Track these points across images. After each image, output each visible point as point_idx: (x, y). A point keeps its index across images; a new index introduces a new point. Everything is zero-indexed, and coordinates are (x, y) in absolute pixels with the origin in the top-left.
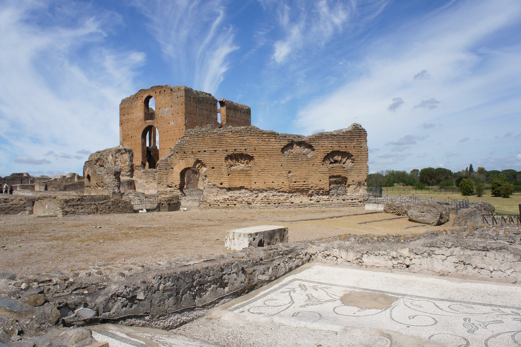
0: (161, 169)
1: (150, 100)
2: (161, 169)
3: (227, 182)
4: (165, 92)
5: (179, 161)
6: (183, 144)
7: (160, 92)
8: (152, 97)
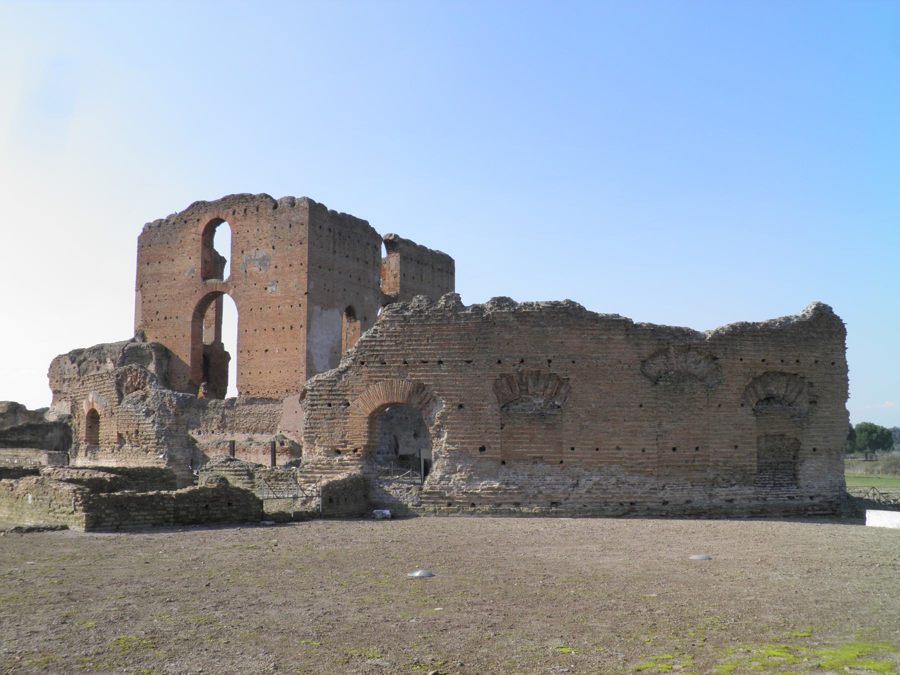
0: (317, 405)
1: (217, 229)
2: (317, 405)
3: (498, 446)
4: (258, 210)
5: (368, 386)
6: (381, 341)
7: (245, 210)
8: (223, 221)
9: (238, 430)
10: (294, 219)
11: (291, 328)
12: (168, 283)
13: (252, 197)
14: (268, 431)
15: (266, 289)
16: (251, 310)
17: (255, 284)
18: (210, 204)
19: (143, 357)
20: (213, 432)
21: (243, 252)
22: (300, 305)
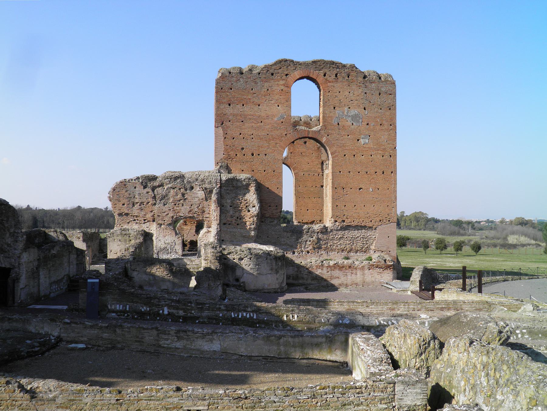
4: (348, 77)
7: (336, 75)
9: (332, 250)
10: (383, 89)
11: (383, 173)
12: (253, 124)
13: (344, 66)
14: (362, 251)
15: (358, 140)
16: (345, 155)
17: (348, 136)
18: (300, 64)
19: (237, 188)
20: (308, 252)
21: (334, 108)
22: (391, 156)
